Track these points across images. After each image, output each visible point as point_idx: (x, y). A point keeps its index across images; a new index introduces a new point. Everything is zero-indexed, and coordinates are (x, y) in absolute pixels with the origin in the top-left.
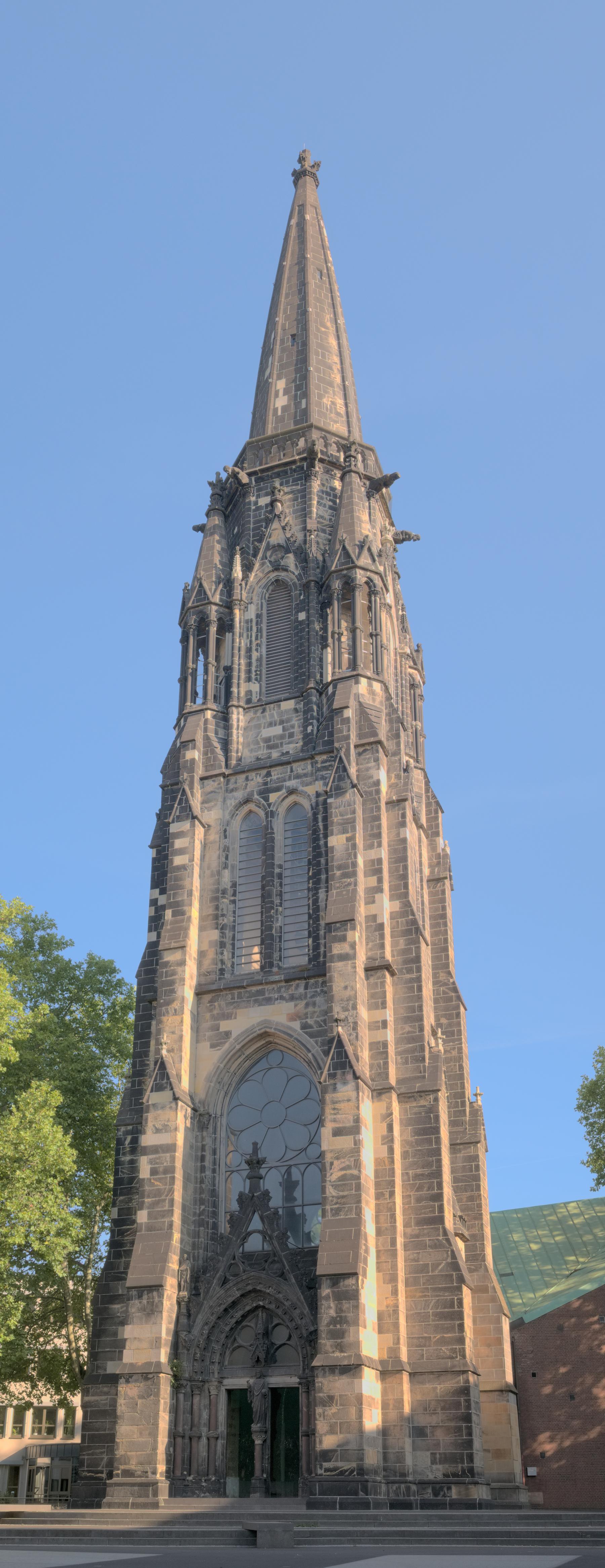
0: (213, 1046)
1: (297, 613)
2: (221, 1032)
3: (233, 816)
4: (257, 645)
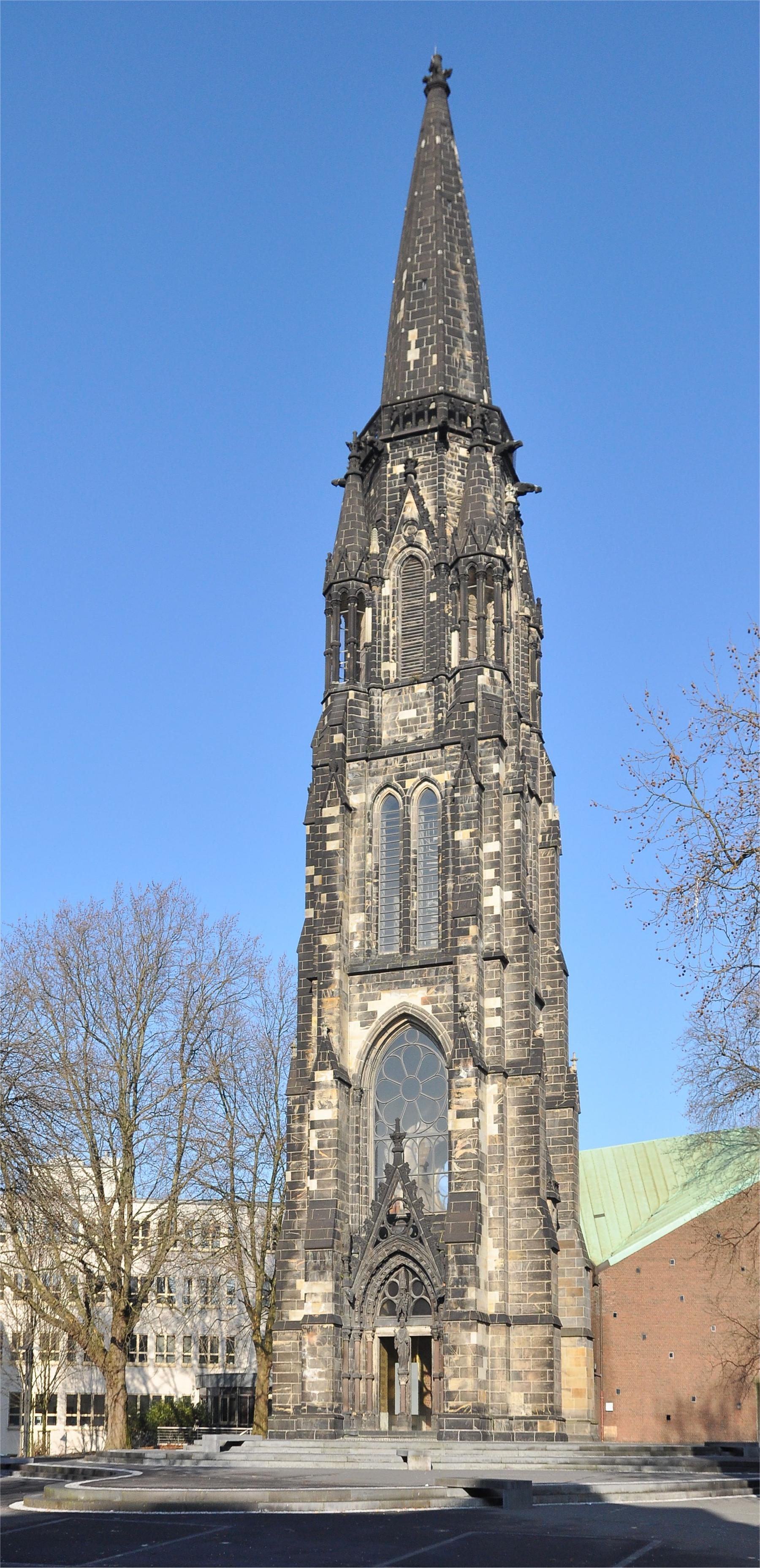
0: (362, 1025)
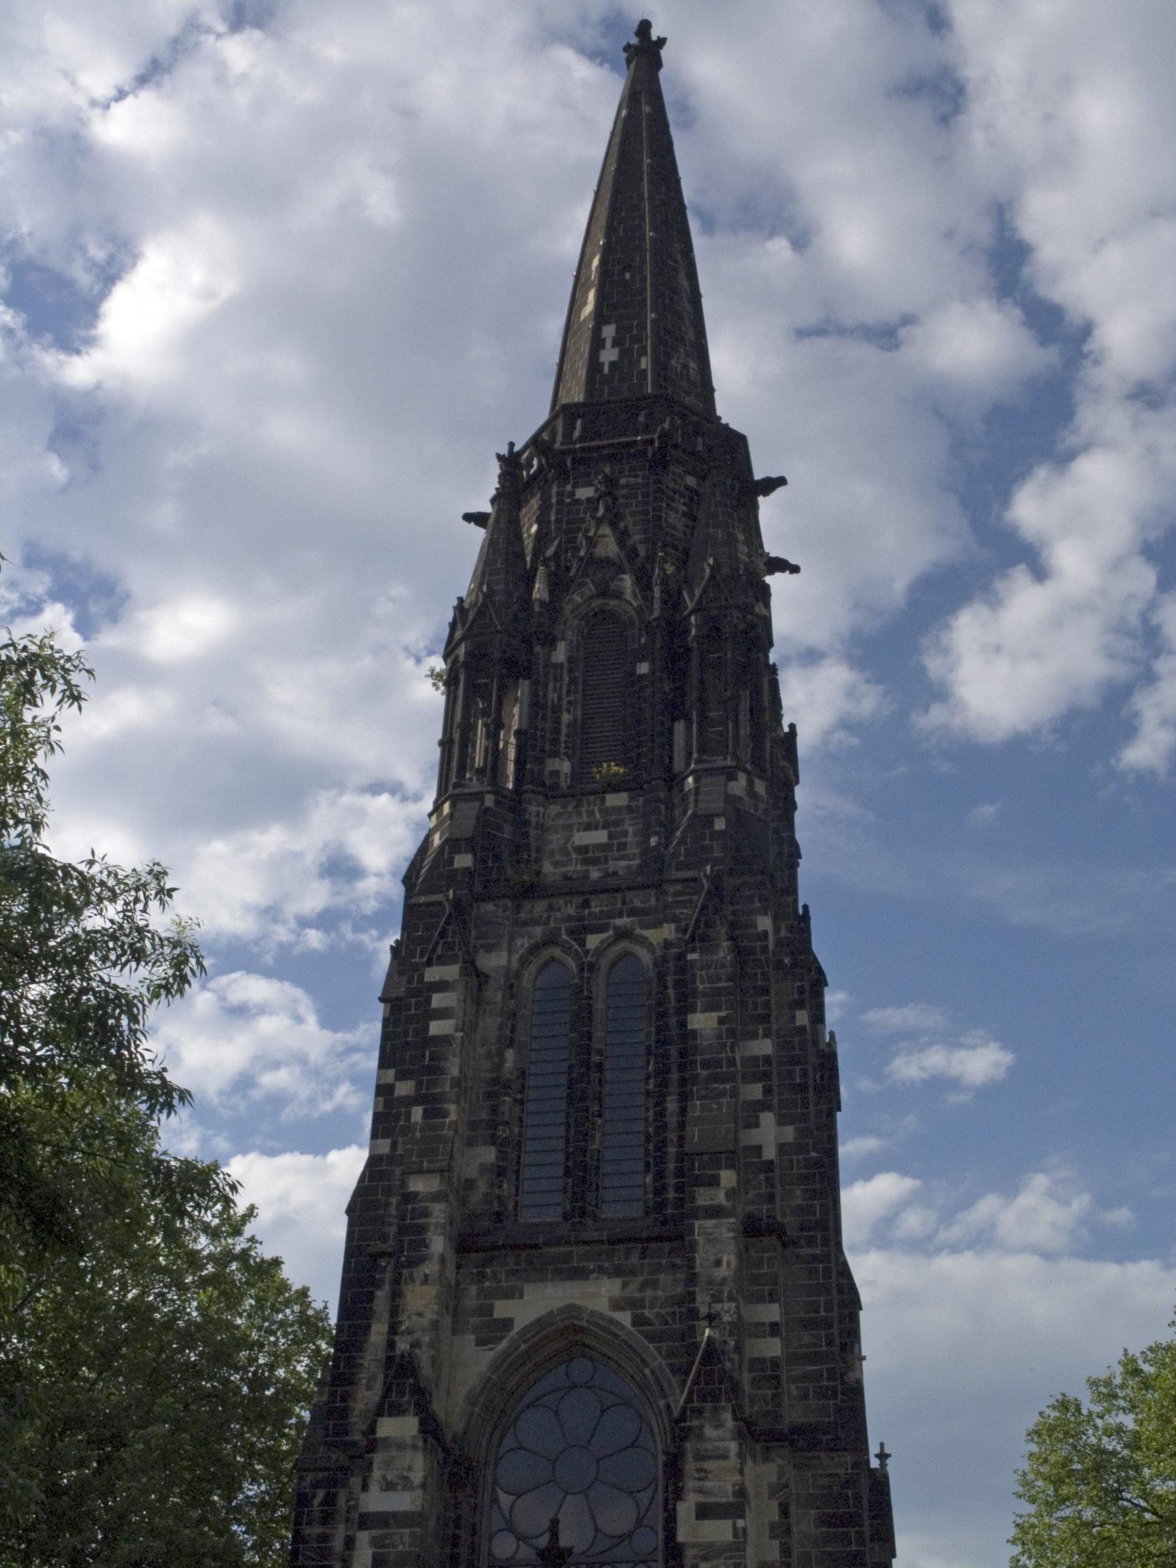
0: (480, 1342)
1: (634, 664)
2: (496, 1319)
3: (524, 962)
4: (570, 702)
